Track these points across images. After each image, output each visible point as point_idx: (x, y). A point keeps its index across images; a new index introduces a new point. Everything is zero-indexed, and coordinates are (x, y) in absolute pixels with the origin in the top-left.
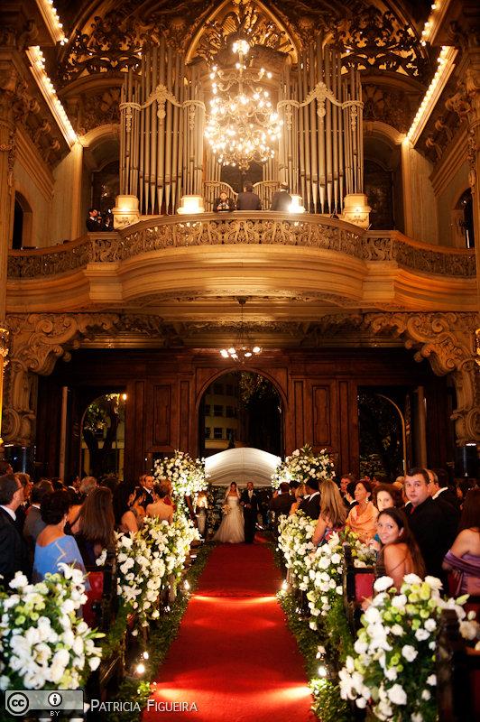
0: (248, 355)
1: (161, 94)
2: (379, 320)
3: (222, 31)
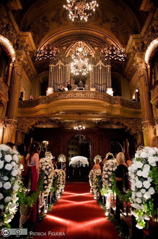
0: (81, 129)
1: (60, 63)
2: (116, 120)
3: (75, 50)
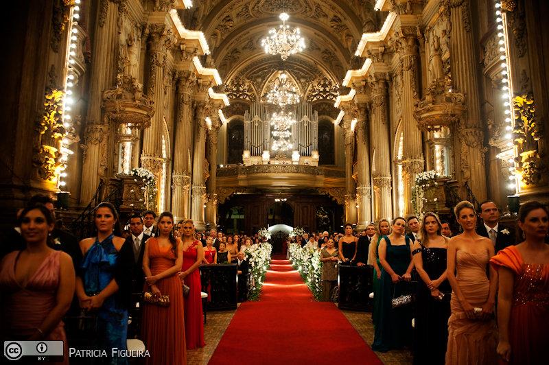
1: (257, 118)
